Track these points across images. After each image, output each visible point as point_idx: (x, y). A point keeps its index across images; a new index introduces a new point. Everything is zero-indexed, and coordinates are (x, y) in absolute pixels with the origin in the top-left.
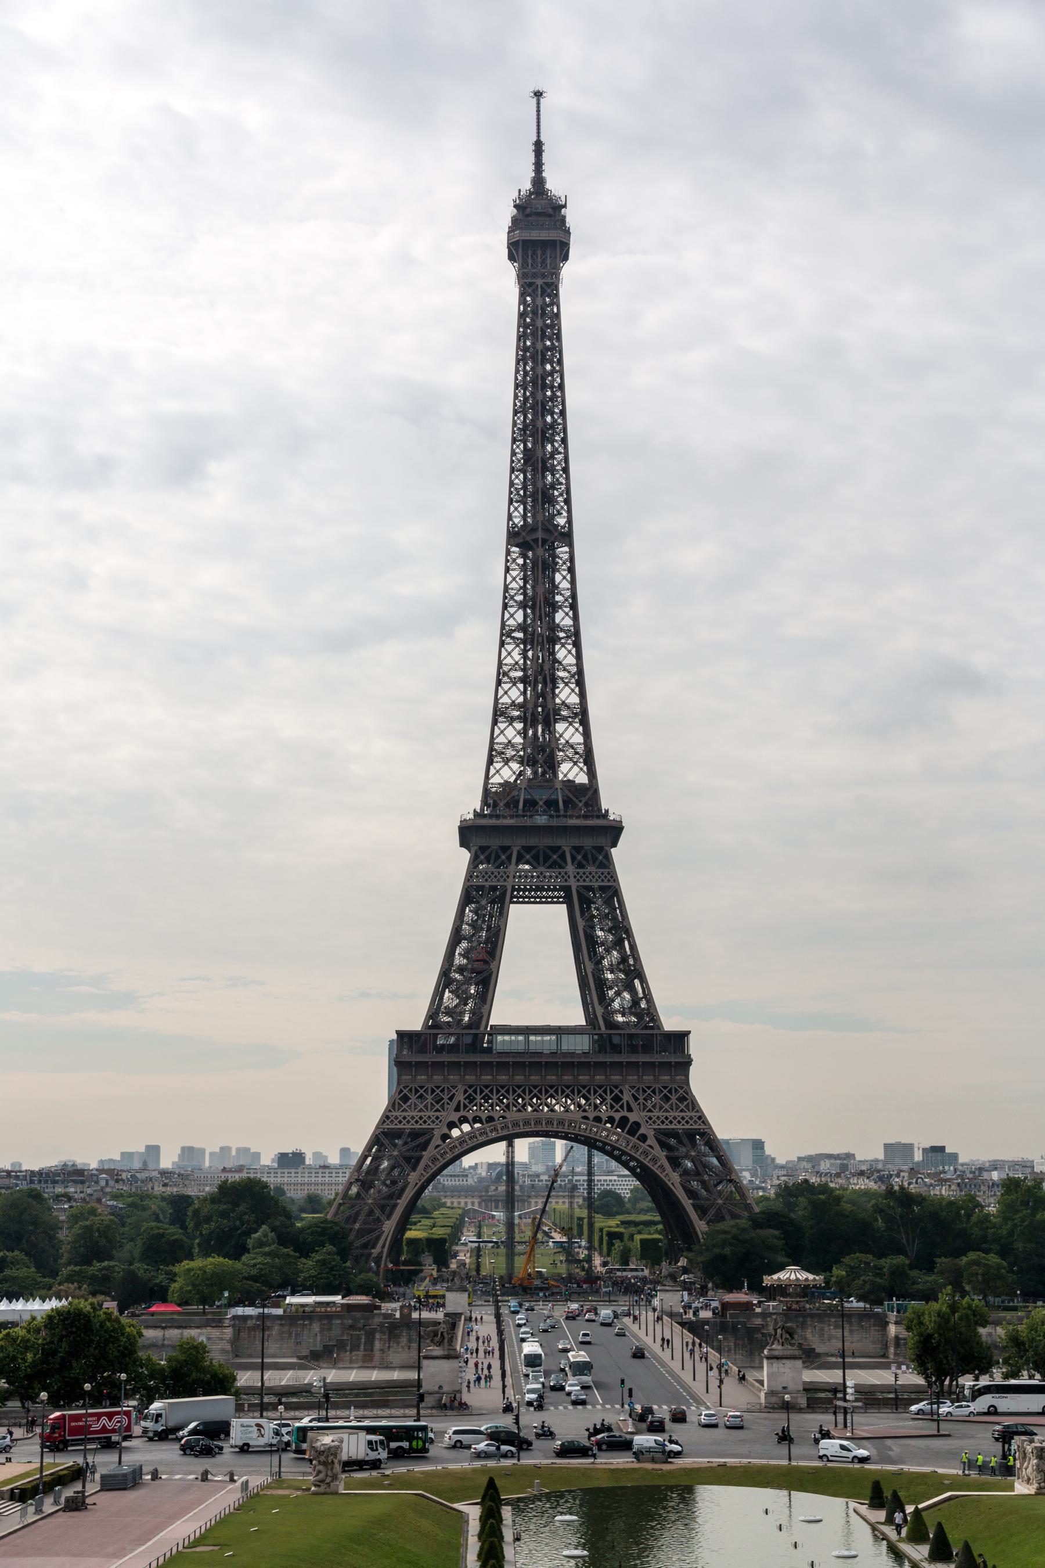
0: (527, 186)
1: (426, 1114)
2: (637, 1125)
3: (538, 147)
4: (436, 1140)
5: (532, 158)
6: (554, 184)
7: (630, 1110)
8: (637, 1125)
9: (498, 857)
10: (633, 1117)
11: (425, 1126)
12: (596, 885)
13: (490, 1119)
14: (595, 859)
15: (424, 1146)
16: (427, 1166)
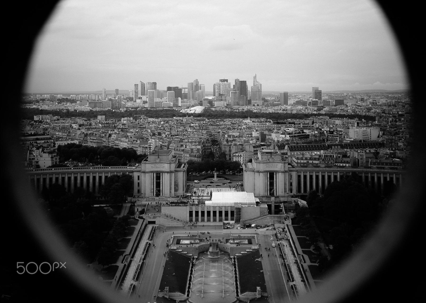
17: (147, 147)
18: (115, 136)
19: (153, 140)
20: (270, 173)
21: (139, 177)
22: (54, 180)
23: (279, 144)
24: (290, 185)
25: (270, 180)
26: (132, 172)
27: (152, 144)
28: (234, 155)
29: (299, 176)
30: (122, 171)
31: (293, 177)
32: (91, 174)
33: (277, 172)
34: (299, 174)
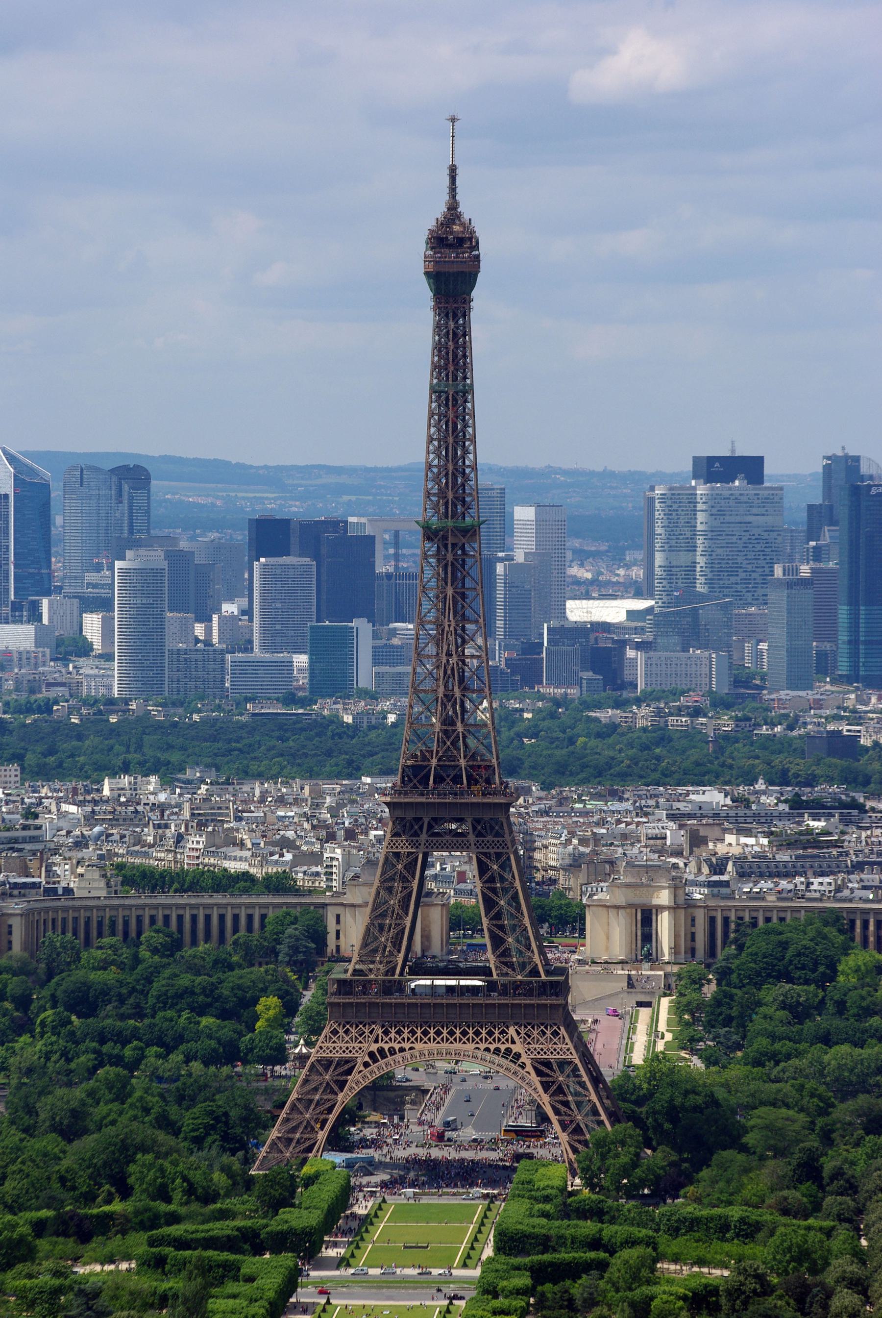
0: (439, 210)
1: (351, 1045)
2: (518, 1056)
3: (453, 170)
4: (359, 1067)
5: (447, 181)
6: (466, 210)
7: (513, 1042)
8: (518, 1056)
9: (412, 827)
10: (516, 1048)
11: (350, 1055)
12: (492, 851)
13: (402, 1050)
14: (492, 828)
15: (349, 1072)
16: (351, 1088)
17: (318, 874)
18: (204, 839)
19: (338, 851)
20: (643, 911)
21: (338, 916)
22: (147, 921)
23: (714, 860)
24: (689, 936)
25: (642, 926)
26: (324, 906)
27: (335, 863)
28: (584, 889)
29: (712, 920)
30: (301, 904)
31: (697, 921)
32: (229, 908)
33: (660, 908)
34: (713, 914)
